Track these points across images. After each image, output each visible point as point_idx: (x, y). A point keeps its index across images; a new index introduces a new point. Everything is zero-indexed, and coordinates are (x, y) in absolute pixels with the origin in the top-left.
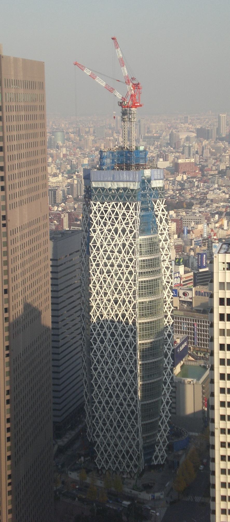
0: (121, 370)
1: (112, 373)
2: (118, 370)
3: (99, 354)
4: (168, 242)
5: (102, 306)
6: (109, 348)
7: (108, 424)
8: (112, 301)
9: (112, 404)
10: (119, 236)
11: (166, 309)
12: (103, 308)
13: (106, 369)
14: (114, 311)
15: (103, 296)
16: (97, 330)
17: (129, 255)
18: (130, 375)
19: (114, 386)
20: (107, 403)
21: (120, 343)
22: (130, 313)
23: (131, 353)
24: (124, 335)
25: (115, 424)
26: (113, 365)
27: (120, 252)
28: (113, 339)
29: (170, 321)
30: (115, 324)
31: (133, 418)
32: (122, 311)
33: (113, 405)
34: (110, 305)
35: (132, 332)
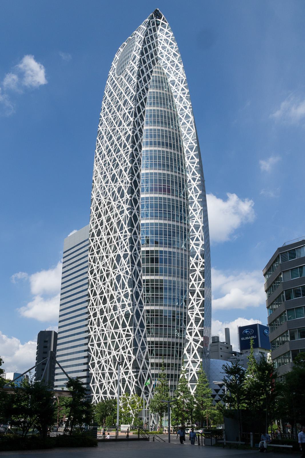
0: (115, 259)
1: (106, 269)
2: (113, 261)
4: (191, 120)
7: (103, 344)
9: (107, 311)
13: (101, 267)
14: (111, 190)
17: (128, 121)
19: (108, 286)
20: (102, 312)
21: (115, 225)
23: (126, 232)
24: (118, 213)
25: (109, 341)
26: (107, 257)
29: (197, 208)
31: (127, 324)
33: (107, 313)
35: (126, 204)
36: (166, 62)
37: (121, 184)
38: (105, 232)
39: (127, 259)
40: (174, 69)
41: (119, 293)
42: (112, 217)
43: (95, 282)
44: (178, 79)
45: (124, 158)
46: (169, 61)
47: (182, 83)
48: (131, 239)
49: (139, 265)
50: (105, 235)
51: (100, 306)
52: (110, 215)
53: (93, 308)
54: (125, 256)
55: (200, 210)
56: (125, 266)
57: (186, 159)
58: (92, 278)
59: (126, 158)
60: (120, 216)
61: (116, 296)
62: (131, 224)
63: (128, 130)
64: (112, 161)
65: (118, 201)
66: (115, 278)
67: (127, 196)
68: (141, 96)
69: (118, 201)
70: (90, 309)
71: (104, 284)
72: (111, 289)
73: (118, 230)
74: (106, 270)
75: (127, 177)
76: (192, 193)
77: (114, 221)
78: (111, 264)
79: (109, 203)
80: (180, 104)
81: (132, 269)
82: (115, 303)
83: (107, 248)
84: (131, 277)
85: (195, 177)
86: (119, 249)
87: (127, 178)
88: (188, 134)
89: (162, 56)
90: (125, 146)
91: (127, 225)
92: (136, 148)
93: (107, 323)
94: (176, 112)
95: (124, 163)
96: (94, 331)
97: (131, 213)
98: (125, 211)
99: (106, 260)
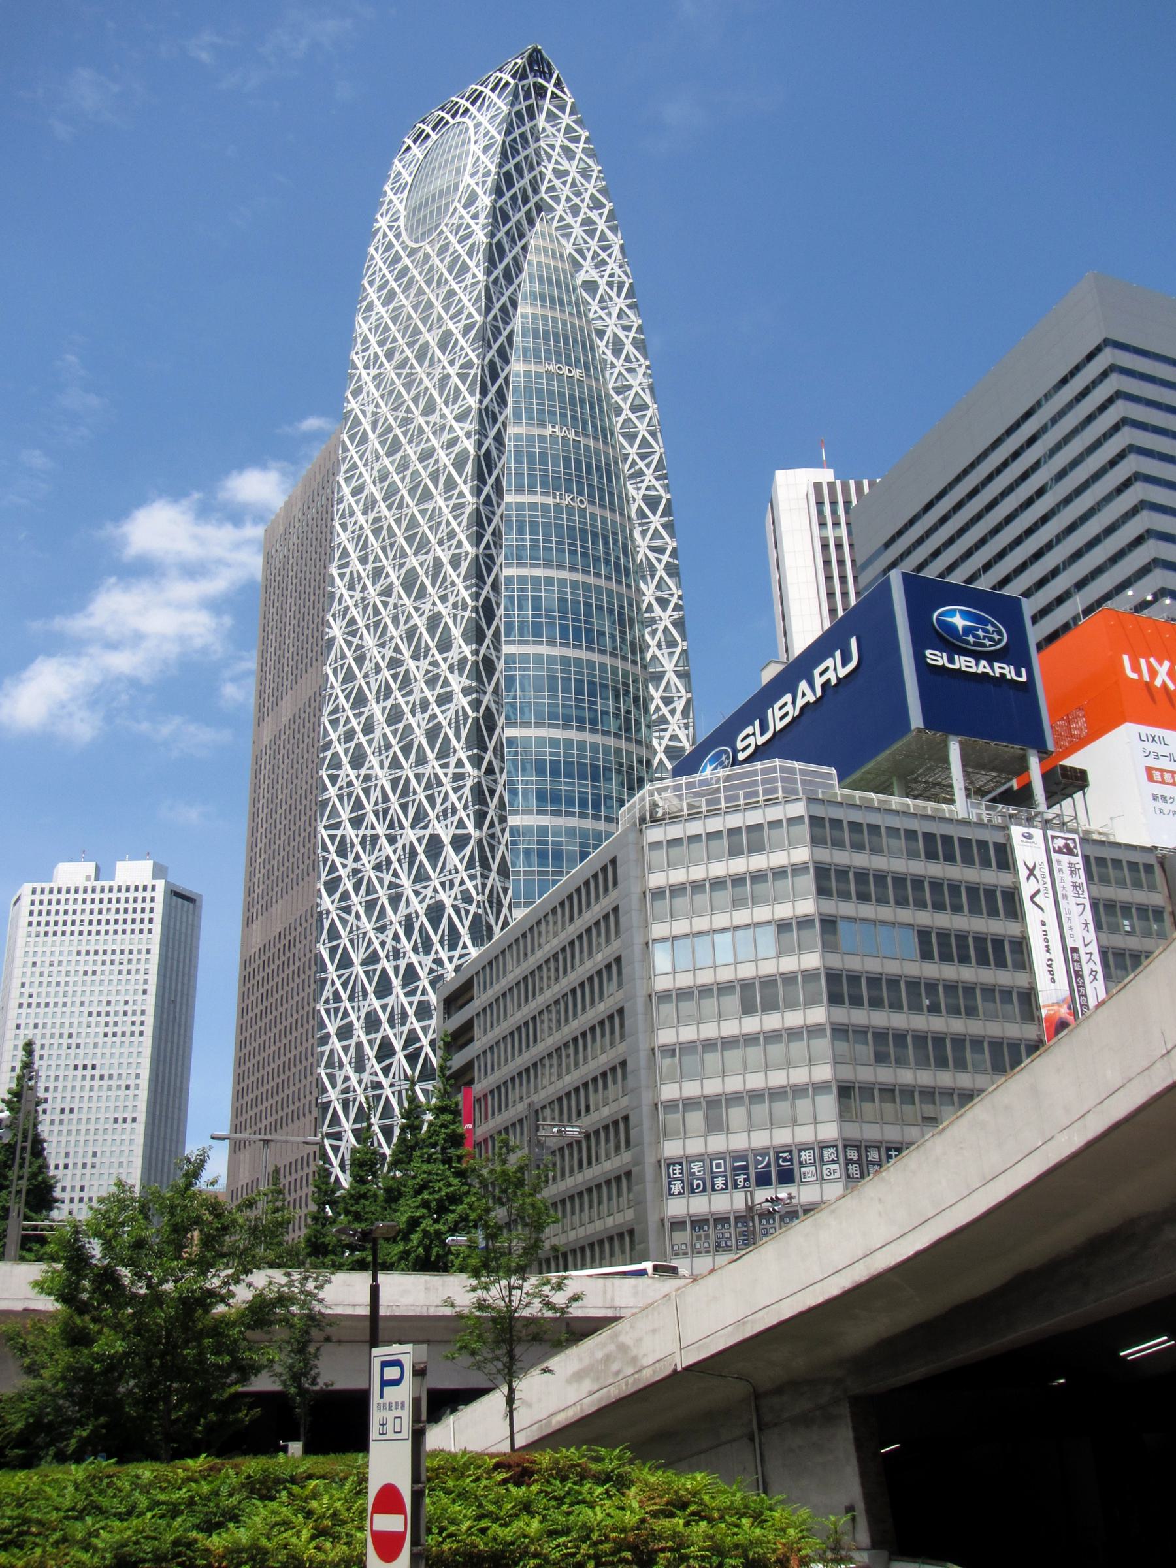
1: (388, 878)
2: (413, 854)
3: (345, 814)
4: (649, 413)
5: (361, 623)
6: (383, 778)
8: (398, 588)
9: (391, 1021)
10: (431, 364)
11: (653, 650)
12: (367, 627)
14: (402, 620)
15: (369, 583)
16: (342, 721)
17: (459, 403)
18: (456, 860)
19: (396, 938)
20: (372, 1023)
22: (455, 606)
23: (460, 764)
24: (432, 700)
26: (392, 840)
27: (429, 409)
28: (394, 733)
30: (402, 670)
32: (428, 606)
34: (391, 606)
35: (461, 675)
36: (569, 219)
37: (440, 607)
38: (383, 757)
39: (468, 850)
40: (594, 244)
41: (438, 962)
42: (406, 709)
43: (344, 922)
44: (606, 278)
45: (448, 523)
46: (579, 219)
47: (619, 295)
48: (478, 790)
49: (503, 871)
50: (382, 767)
51: (366, 1003)
52: (401, 701)
53: (337, 1010)
54: (459, 842)
55: (684, 701)
56: (459, 876)
57: (637, 535)
58: (331, 908)
59: (454, 524)
60: (437, 711)
61: (427, 970)
62: (477, 741)
63: (461, 433)
64: (404, 526)
65: (429, 659)
66: (421, 912)
67: (463, 649)
68: (498, 329)
69: (429, 659)
70: (327, 1011)
71: (382, 929)
72: (406, 945)
73: (431, 755)
74: (386, 884)
75: (460, 586)
76: (659, 646)
77: (418, 724)
78: (406, 866)
79: (394, 663)
80: (615, 361)
81: (484, 885)
82: (424, 992)
83: (391, 812)
84: (480, 911)
85: (665, 595)
86: (438, 817)
87: (462, 590)
88: (643, 457)
89: (556, 199)
90: (450, 484)
91: (463, 740)
92: (488, 496)
93: (395, 1060)
94: (605, 383)
95: (449, 539)
96: (340, 1086)
97: (476, 705)
98: (455, 698)
99: (389, 850)
